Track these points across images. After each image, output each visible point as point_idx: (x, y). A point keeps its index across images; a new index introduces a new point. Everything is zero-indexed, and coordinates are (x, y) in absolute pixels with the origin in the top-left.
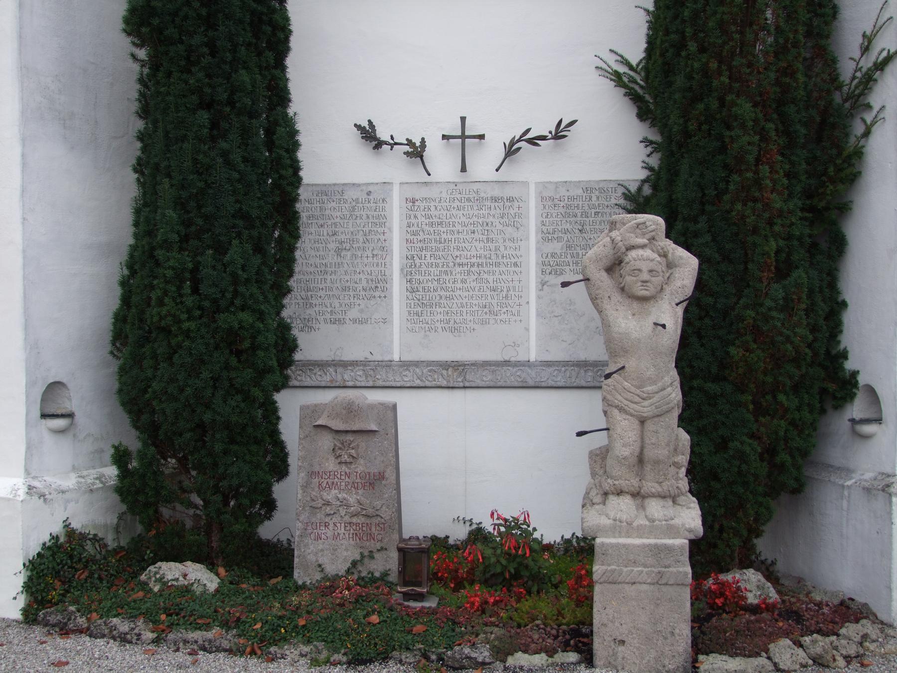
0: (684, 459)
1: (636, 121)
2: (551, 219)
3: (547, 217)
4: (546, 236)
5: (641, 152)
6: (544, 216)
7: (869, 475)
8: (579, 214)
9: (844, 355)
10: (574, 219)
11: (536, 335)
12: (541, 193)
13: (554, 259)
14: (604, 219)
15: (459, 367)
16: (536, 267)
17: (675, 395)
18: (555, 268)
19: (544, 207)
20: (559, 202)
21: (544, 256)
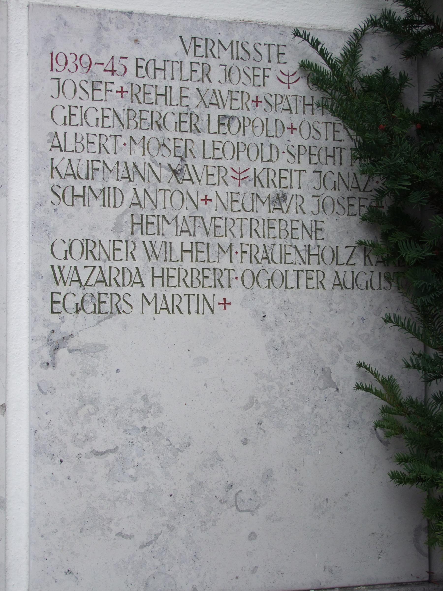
2: (83, 130)
3: (68, 121)
6: (59, 118)
8: (171, 120)
10: (155, 133)
11: (31, 522)
12: (48, 40)
13: (91, 262)
14: (248, 139)
16: (32, 286)
18: (95, 290)
19: (61, 89)
20: (108, 77)
21: (60, 250)
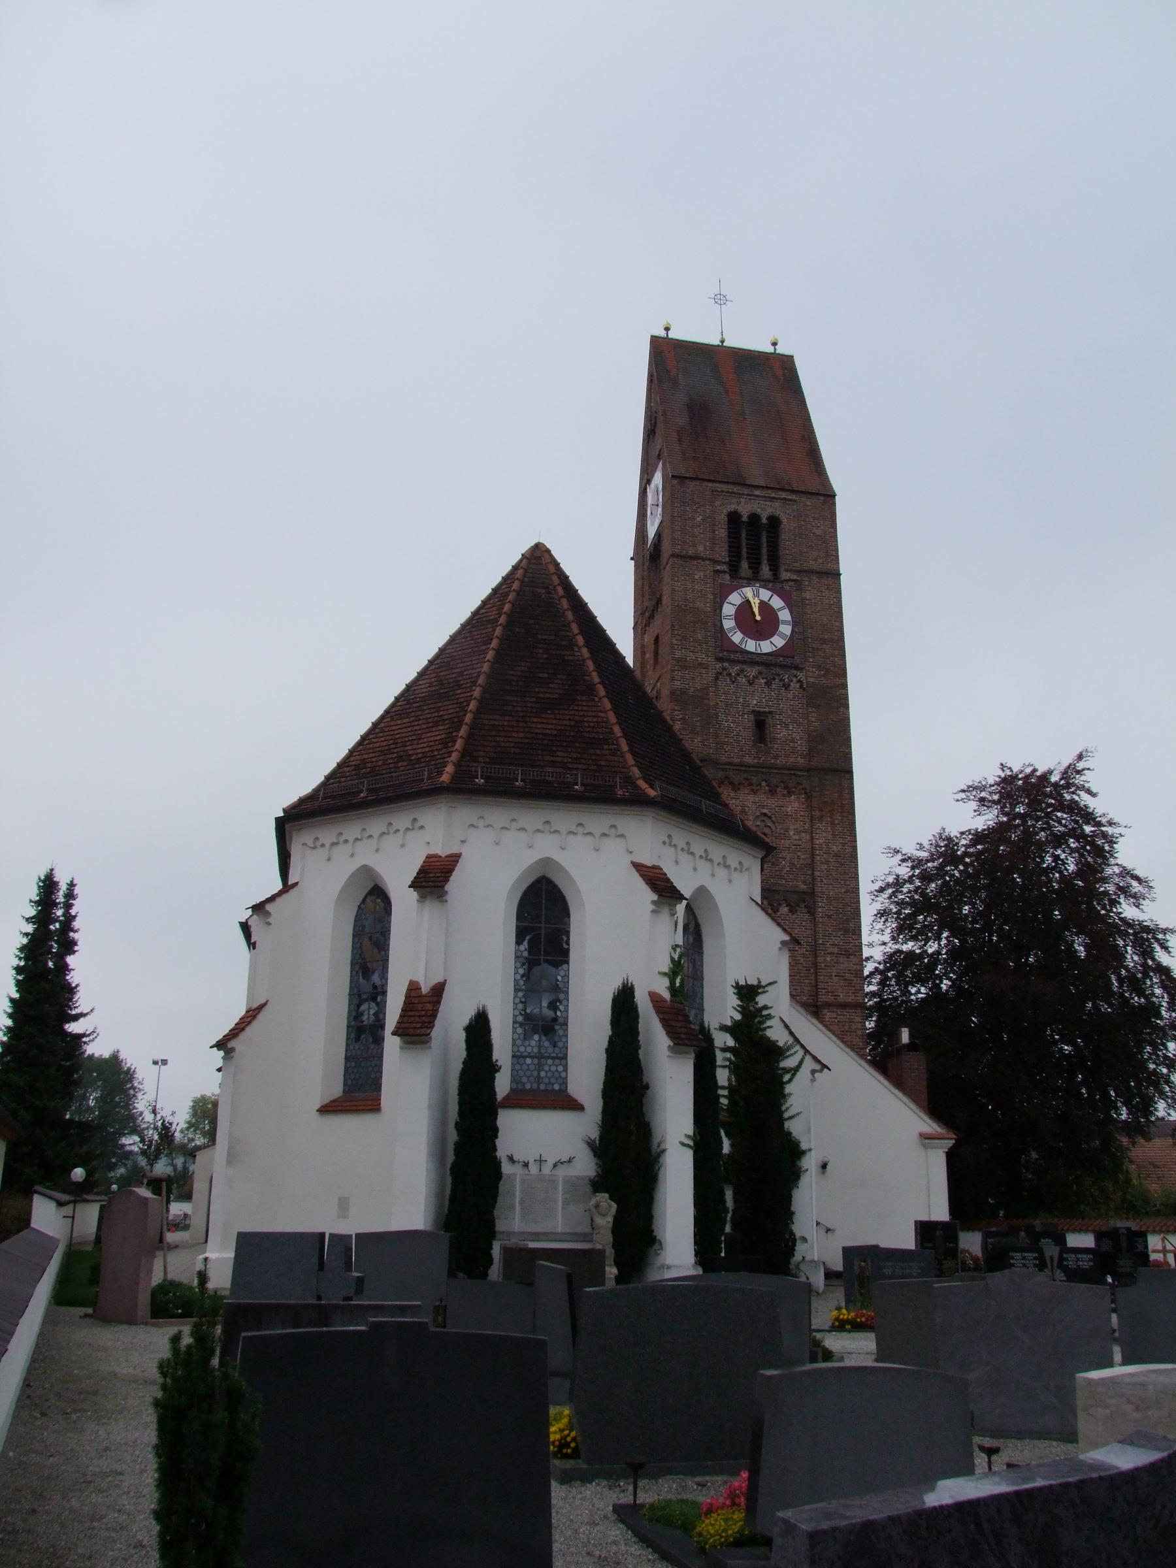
0: (613, 1256)
1: (593, 1158)
4: (564, 1193)
5: (595, 1167)
7: (659, 1265)
9: (653, 1231)
15: (537, 1234)
17: (611, 1240)
